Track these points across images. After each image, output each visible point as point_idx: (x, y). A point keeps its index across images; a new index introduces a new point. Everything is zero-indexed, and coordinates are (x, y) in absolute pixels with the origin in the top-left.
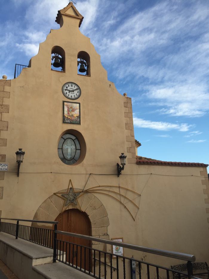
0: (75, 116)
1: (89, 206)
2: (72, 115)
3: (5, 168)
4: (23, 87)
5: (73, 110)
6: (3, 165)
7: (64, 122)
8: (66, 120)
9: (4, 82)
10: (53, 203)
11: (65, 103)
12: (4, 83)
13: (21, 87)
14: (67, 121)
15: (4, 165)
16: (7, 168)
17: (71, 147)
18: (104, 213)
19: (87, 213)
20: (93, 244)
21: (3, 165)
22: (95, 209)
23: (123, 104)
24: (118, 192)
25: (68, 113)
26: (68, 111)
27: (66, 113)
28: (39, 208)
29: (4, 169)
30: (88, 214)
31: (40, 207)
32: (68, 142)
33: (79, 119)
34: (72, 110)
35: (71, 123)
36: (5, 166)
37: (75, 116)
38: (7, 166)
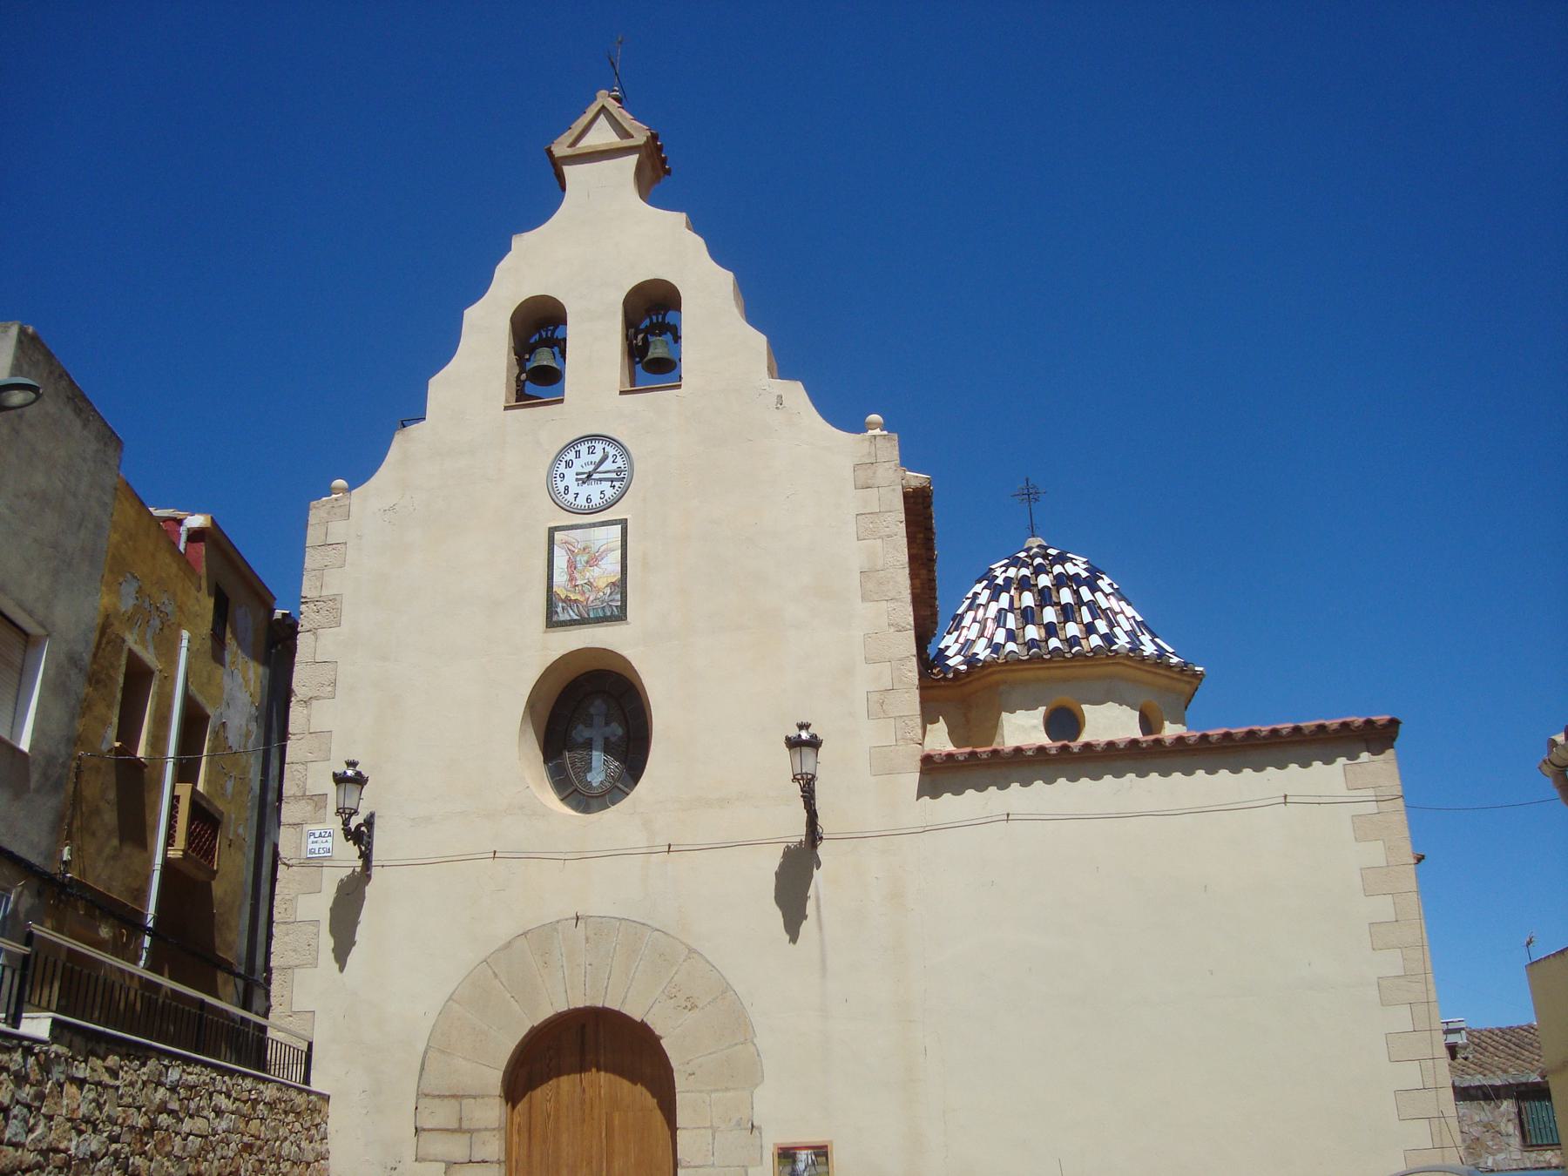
0: (602, 583)
1: (663, 992)
2: (590, 584)
3: (322, 846)
4: (392, 508)
5: (593, 561)
6: (317, 835)
7: (552, 623)
8: (559, 610)
9: (329, 506)
10: (503, 980)
11: (558, 536)
12: (329, 513)
13: (385, 510)
14: (563, 617)
15: (320, 836)
16: (329, 845)
17: (608, 731)
18: (738, 1025)
19: (652, 1027)
20: (684, 1164)
21: (317, 835)
22: (694, 1007)
23: (848, 474)
24: (242, 970)
25: (572, 579)
26: (572, 566)
27: (560, 578)
28: (447, 1001)
29: (321, 851)
30: (657, 1033)
31: (450, 998)
32: (592, 710)
33: (618, 597)
34: (587, 562)
35: (583, 621)
36: (324, 840)
37: (602, 583)
38: (330, 839)
